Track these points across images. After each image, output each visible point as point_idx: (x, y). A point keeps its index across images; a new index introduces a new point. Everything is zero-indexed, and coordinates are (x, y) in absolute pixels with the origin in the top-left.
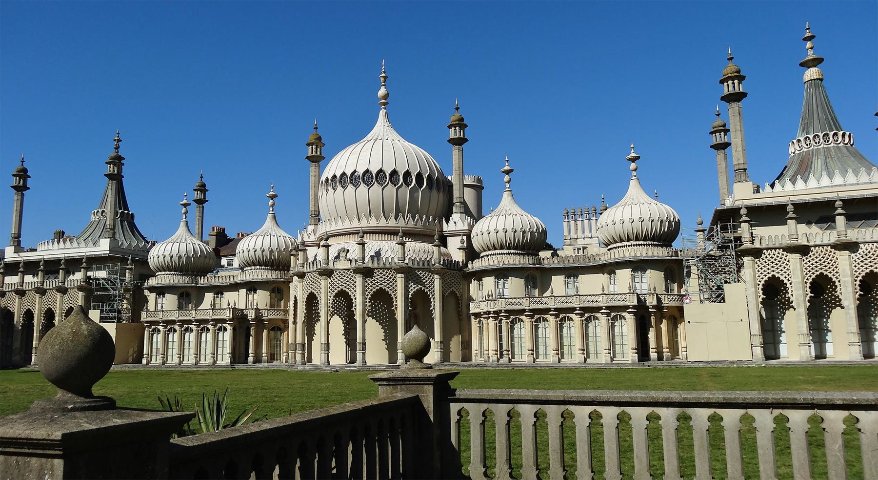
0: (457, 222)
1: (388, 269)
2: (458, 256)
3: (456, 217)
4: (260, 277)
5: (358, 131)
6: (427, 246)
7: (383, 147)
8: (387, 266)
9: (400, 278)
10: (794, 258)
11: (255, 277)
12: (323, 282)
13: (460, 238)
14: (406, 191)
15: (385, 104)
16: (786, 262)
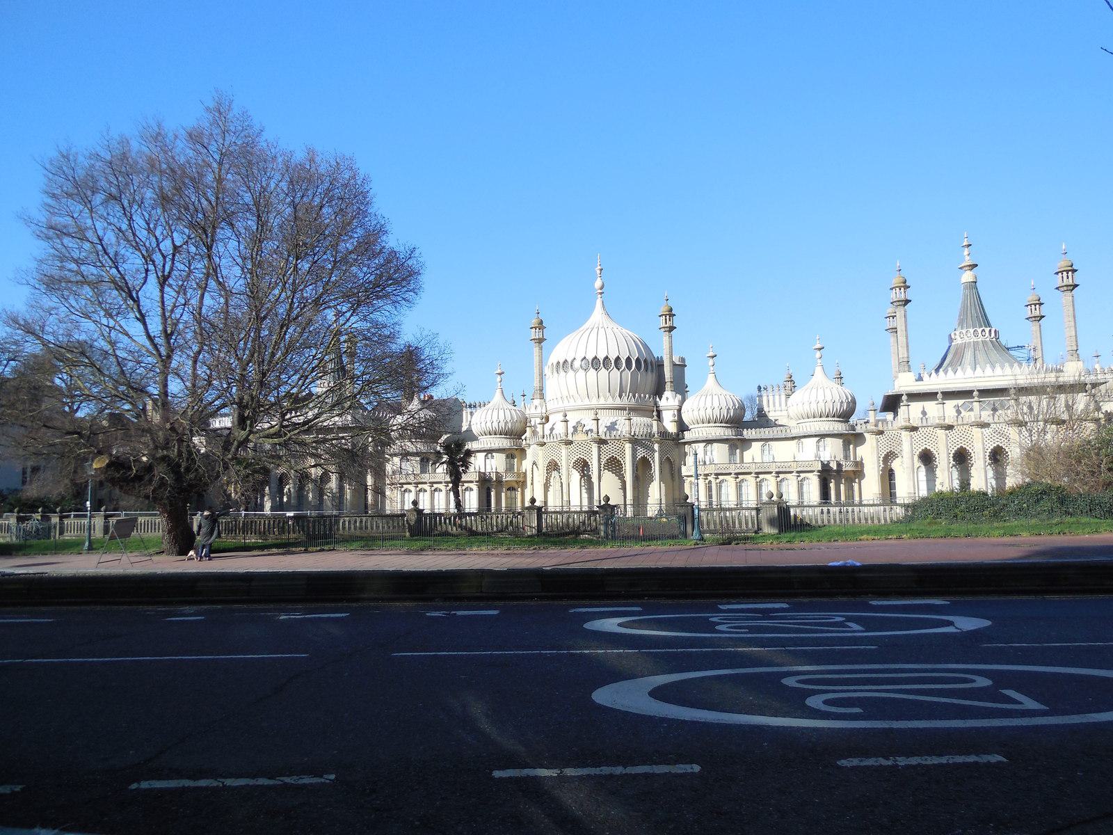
0: (668, 400)
1: (618, 440)
2: (671, 428)
3: (668, 394)
4: (497, 445)
5: (578, 318)
6: (647, 420)
7: (602, 334)
8: (618, 438)
9: (628, 447)
10: (941, 433)
11: (493, 445)
12: (564, 450)
13: (672, 412)
14: (628, 374)
15: (601, 293)
16: (935, 437)
